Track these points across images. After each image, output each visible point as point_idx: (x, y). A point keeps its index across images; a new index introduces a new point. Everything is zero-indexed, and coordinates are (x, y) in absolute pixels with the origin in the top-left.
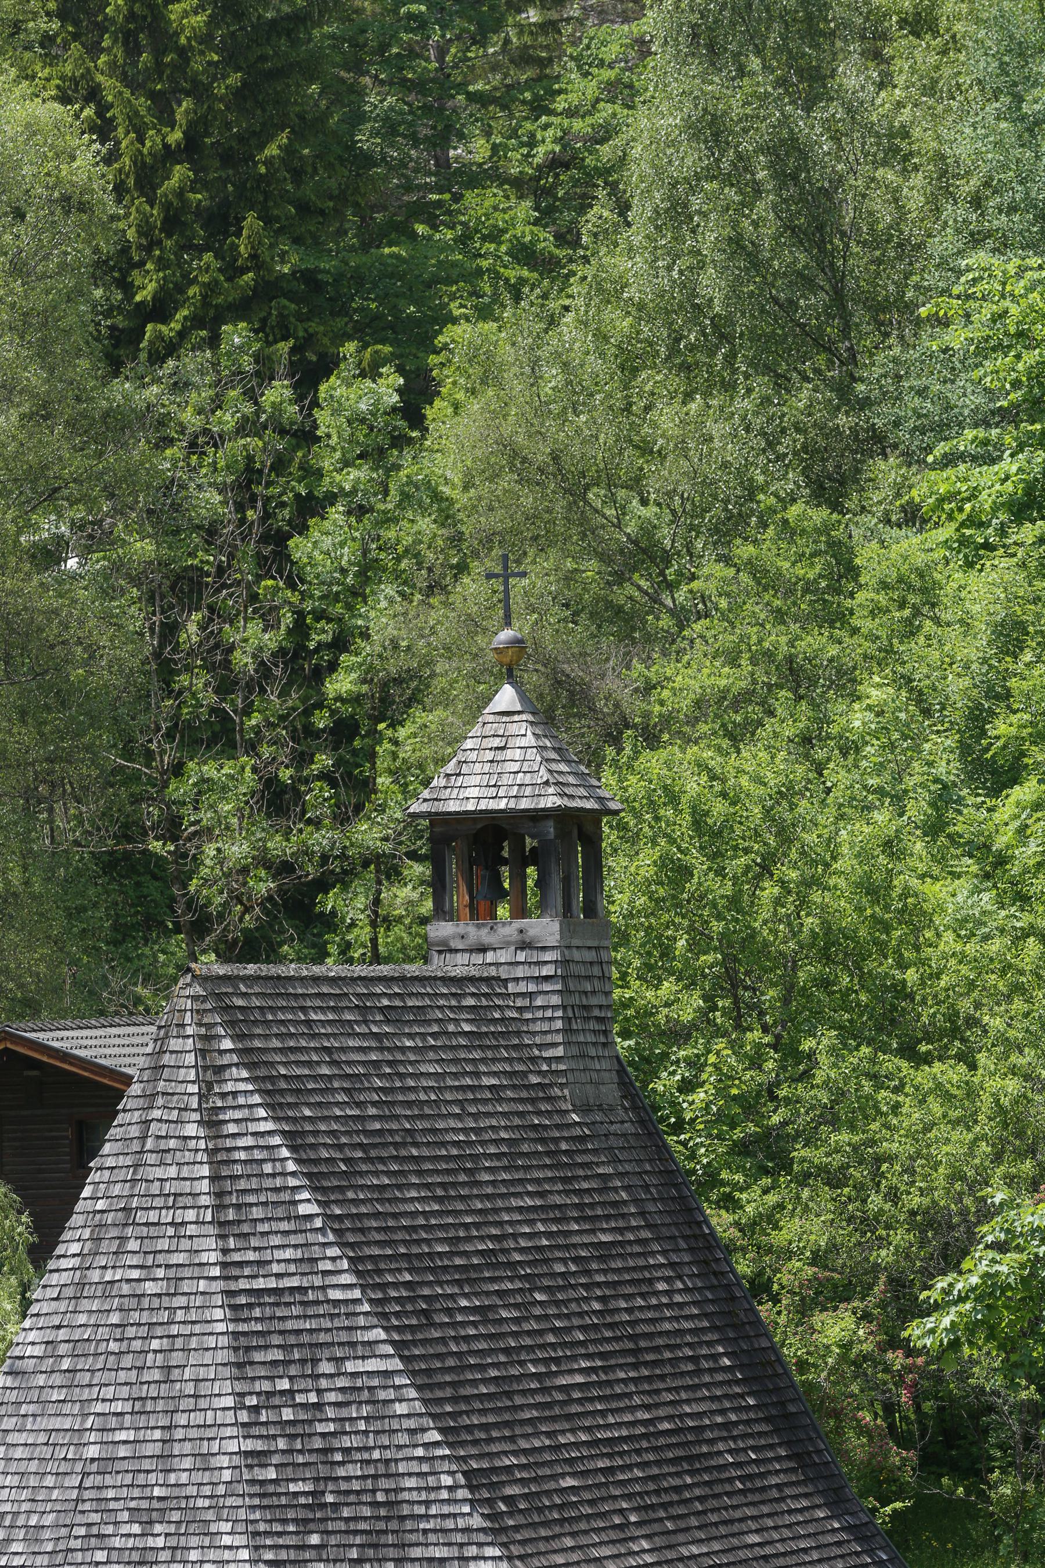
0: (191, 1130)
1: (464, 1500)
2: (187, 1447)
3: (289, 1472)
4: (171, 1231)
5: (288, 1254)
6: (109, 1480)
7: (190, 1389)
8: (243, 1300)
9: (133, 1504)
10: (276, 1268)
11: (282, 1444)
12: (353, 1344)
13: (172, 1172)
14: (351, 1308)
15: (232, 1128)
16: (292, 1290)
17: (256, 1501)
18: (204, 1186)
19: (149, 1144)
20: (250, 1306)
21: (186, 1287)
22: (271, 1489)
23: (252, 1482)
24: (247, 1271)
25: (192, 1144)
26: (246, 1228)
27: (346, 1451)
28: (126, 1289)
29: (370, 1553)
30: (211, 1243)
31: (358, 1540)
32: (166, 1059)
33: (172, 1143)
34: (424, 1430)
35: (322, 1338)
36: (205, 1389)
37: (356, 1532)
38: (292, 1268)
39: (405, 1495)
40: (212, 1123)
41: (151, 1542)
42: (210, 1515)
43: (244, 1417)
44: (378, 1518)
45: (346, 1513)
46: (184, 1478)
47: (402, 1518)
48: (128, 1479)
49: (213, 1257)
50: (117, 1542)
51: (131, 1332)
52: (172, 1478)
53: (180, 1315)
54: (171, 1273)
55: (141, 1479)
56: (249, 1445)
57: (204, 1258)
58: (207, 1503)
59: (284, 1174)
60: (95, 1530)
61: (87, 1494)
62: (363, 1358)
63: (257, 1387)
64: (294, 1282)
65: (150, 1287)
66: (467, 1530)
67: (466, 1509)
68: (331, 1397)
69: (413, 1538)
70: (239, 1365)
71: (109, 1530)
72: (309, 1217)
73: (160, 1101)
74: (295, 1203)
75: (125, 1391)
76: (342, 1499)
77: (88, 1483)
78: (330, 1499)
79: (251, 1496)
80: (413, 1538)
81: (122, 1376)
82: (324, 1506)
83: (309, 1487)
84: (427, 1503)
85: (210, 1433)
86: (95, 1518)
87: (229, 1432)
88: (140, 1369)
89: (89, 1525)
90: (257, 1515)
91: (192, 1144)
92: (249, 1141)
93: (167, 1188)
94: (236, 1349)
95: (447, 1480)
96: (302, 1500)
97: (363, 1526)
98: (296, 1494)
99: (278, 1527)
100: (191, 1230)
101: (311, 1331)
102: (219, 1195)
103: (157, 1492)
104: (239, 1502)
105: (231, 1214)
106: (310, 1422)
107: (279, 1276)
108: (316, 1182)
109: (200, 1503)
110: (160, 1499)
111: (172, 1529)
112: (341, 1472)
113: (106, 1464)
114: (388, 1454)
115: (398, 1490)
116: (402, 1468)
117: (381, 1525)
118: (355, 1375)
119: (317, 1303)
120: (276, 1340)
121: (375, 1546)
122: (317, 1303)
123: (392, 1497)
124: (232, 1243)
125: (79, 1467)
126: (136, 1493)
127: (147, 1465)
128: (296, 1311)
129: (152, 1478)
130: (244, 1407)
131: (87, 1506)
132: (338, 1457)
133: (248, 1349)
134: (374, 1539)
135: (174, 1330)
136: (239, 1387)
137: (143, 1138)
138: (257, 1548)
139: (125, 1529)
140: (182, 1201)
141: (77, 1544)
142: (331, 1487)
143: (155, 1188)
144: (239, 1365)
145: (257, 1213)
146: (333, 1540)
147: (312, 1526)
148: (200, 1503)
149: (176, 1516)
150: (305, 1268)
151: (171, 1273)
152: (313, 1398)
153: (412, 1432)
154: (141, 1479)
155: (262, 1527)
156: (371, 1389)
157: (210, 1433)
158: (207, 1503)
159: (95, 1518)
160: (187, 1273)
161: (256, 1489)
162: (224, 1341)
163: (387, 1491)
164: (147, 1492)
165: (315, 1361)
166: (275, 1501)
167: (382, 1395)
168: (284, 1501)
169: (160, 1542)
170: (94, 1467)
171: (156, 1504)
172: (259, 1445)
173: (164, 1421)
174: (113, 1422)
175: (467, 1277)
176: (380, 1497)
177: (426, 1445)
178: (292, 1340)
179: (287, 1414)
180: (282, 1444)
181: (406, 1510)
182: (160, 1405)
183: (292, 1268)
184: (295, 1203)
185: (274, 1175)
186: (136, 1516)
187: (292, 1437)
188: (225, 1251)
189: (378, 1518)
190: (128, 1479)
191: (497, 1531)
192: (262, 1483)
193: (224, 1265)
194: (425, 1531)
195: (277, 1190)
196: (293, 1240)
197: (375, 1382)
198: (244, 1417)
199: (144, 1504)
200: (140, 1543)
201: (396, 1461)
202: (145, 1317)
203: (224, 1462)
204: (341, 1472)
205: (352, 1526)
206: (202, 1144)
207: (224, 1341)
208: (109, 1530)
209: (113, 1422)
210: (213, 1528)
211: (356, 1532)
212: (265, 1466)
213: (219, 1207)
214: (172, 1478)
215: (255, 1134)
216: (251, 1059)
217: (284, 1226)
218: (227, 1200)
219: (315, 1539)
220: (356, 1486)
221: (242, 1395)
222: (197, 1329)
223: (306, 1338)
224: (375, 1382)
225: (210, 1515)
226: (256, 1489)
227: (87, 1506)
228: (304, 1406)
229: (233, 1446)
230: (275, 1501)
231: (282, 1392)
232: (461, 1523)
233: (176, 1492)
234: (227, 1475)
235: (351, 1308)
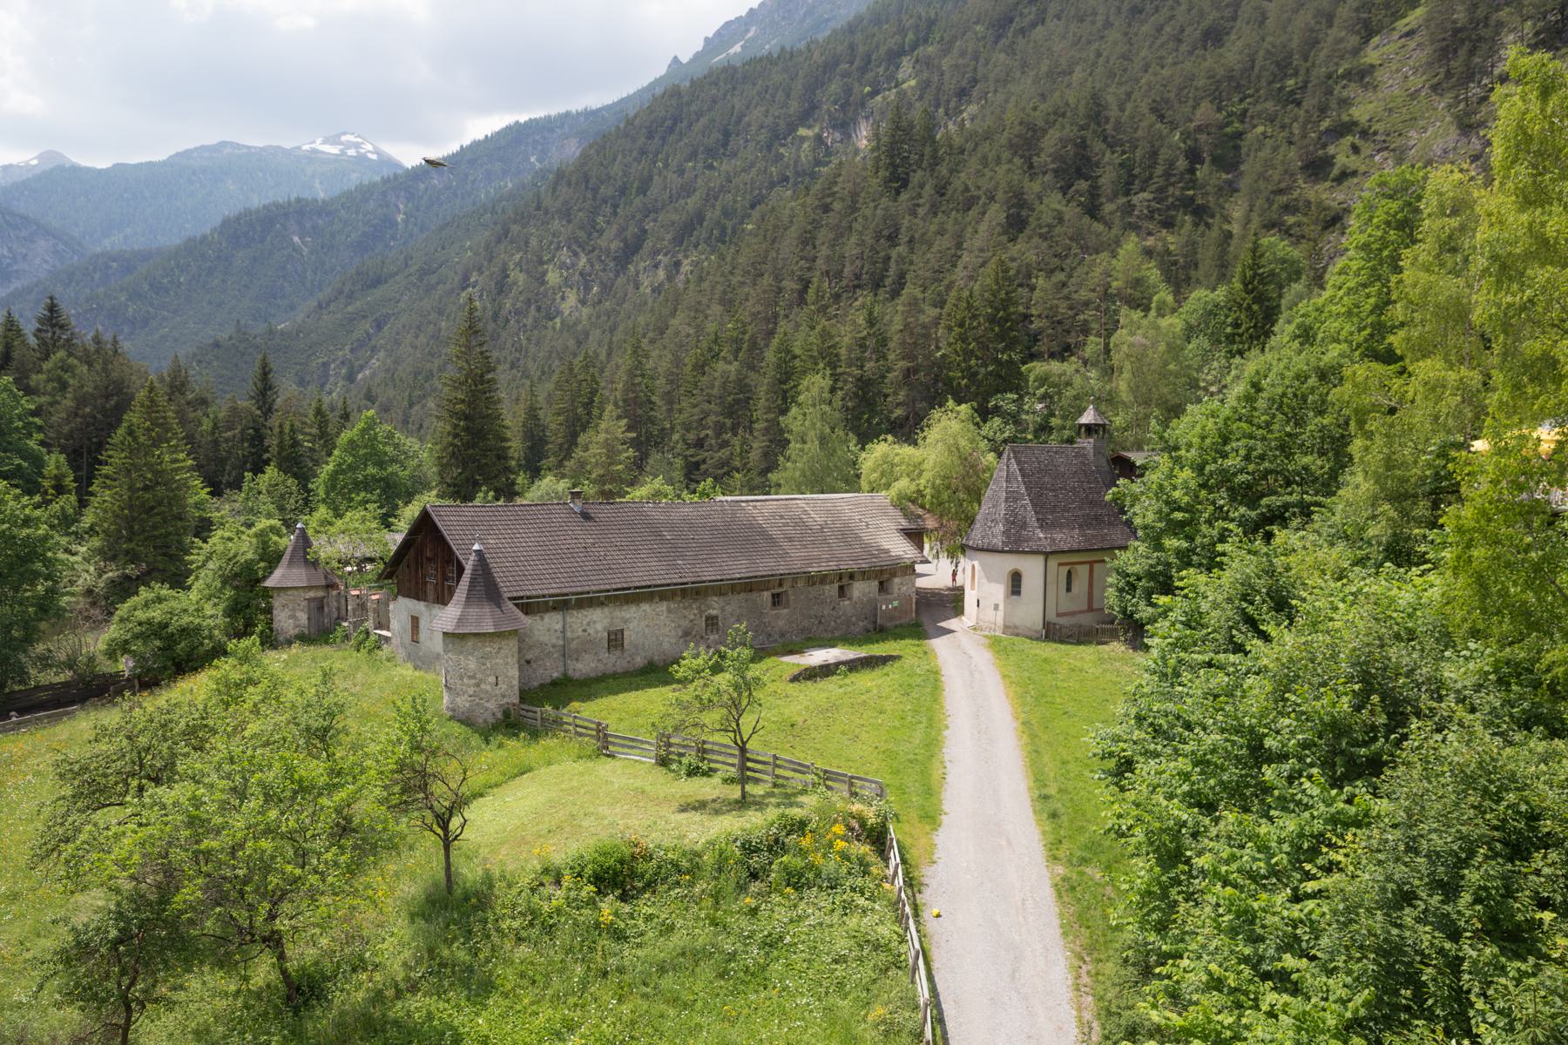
108: (1023, 476)
175: (1052, 491)
191: (1041, 527)
216: (1015, 458)
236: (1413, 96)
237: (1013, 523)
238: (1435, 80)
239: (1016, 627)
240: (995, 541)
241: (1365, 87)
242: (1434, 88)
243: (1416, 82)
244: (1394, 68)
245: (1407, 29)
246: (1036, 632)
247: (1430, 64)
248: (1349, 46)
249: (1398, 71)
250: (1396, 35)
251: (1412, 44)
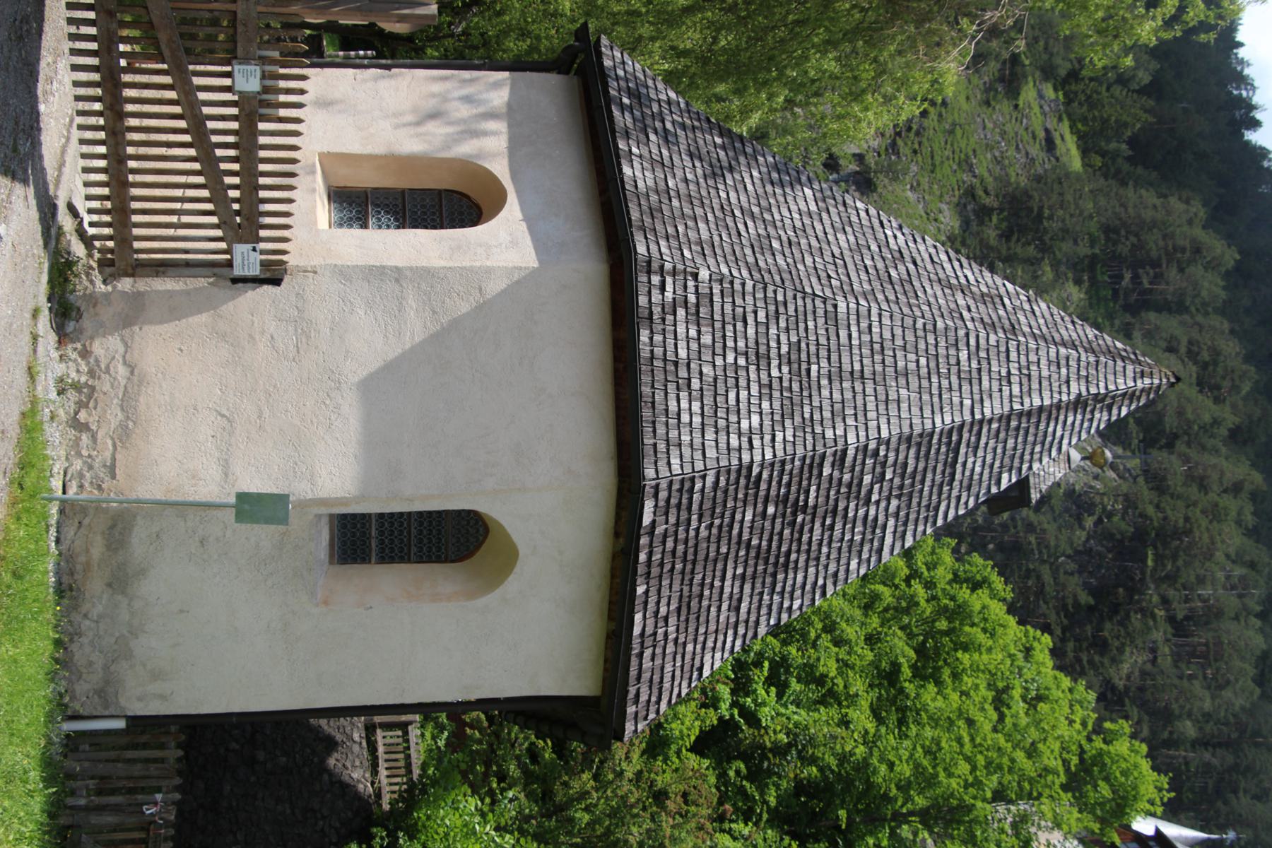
0: (1074, 388)
1: (779, 619)
2: (848, 395)
3: (824, 485)
4: (1004, 372)
5: (978, 469)
6: (821, 321)
7: (893, 396)
8: (954, 438)
9: (803, 345)
10: (971, 460)
11: (847, 477)
12: (906, 524)
13: (1045, 373)
14: (931, 520)
15: (1070, 420)
16: (953, 475)
17: (808, 461)
18: (1037, 402)
19: (1063, 351)
20: (949, 443)
21: (966, 387)
22: (815, 472)
23: (823, 456)
24: (973, 439)
25: (1064, 389)
26: (1002, 435)
27: (832, 527)
28: (961, 333)
29: (753, 554)
30: (997, 411)
31: (764, 543)
32: (1119, 363)
33: (1064, 371)
34: (835, 584)
35: (915, 501)
36: (893, 408)
37: (770, 541)
38: (967, 473)
39: (791, 575)
40: (1079, 404)
41: (775, 363)
42: (798, 419)
43: (872, 445)
44: (778, 557)
45: (787, 532)
46: (825, 393)
47: (774, 575)
48: (823, 341)
49: (987, 412)
50: (773, 331)
51: (931, 339)
52: (824, 382)
53: (945, 383)
54: (975, 374)
55: (823, 353)
56: (851, 452)
57: (987, 404)
58: (807, 416)
59: (1031, 461)
60: (782, 310)
61: (808, 301)
62: (895, 532)
63: (892, 455)
64: (958, 476)
65: (963, 355)
66: (757, 623)
67: (772, 622)
68: (872, 512)
69: (758, 585)
70: (909, 439)
71: (783, 324)
72: (999, 483)
73: (1092, 359)
74: (1010, 471)
75: (887, 335)
76: (797, 527)
77: (818, 302)
78: (799, 519)
79: (813, 457)
80: (758, 585)
81: (898, 331)
82: (794, 514)
83: (811, 501)
84: (782, 593)
85: (861, 418)
86: (791, 311)
87: (862, 434)
88: (904, 348)
89: (785, 304)
90: (797, 463)
91: (1064, 389)
92: (1059, 433)
93: (1034, 368)
94: (921, 435)
95: (796, 604)
96: (802, 497)
97: (774, 544)
98: (807, 492)
99: (786, 478)
100: (1006, 389)
101: (922, 491)
102: (1029, 414)
103: (814, 368)
104: (809, 447)
105: (1014, 423)
106: (858, 498)
107: (964, 464)
109: (807, 409)
110: (809, 371)
111: (786, 384)
112: (817, 525)
113: (832, 317)
114: (823, 559)
115: (796, 569)
116: (812, 570)
117: (772, 560)
118: (884, 527)
119: (940, 494)
120: (921, 466)
121: (757, 557)
122: (940, 494)
123: (792, 565)
124: (995, 426)
125: (828, 293)
126: (813, 349)
127: (834, 357)
128: (938, 478)
129: (824, 363)
130: (879, 444)
131: (800, 302)
132: (828, 522)
133: (919, 445)
134: (763, 555)
135: (934, 379)
136: (894, 440)
137: (1064, 345)
138: (772, 465)
139: (783, 338)
140: (1025, 380)
141: (770, 294)
142: (808, 518)
143: (1033, 358)
144: (909, 439)
145: (1011, 443)
146: (767, 524)
147: (781, 507)
148: (807, 409)
149: (796, 386)
150: (965, 483)
151: (975, 374)
152: (875, 497)
153: (836, 575)
154: (823, 353)
155: (788, 467)
156: (872, 541)
157: (861, 418)
158: (807, 416)
159: (791, 311)
160: (976, 389)
161: (817, 460)
162: (928, 426)
163: (797, 562)
164: (813, 359)
165: (899, 497)
166: (806, 475)
167: (866, 548)
168: (805, 483)
169: (775, 373)
170: (830, 308)
171: (804, 366)
172: (849, 459)
173: (867, 373)
174: (864, 324)
176: (793, 556)
177: (824, 586)
178: (918, 478)
179: (867, 479)
180: (847, 477)
181: (780, 577)
182: (879, 368)
183: (967, 473)
184: (1010, 471)
185: (1032, 453)
186: (794, 348)
187: (850, 485)
188: (990, 421)
189: (778, 557)
190: (823, 341)
192: (821, 465)
193: (981, 422)
194: (761, 594)
195: (1022, 457)
196: (986, 472)
197: (876, 544)
198: (872, 445)
199: (804, 356)
200: (773, 353)
201: (817, 566)
202: (942, 351)
203: (840, 432)
204: (817, 525)
205: (776, 538)
206: (1065, 398)
207: (928, 426)
208: (783, 324)
209: (864, 324)
210: (788, 423)
211: (770, 541)
212: (833, 465)
213: (1020, 414)
214: (824, 382)
215: (1062, 437)
217: (997, 464)
218: (1024, 420)
219: (771, 510)
220: (805, 537)
221: (888, 442)
222: (936, 399)
223: (918, 487)
224: (876, 544)
225: (798, 419)
226: (817, 460)
227: (800, 302)
228: (870, 492)
229: (851, 439)
230: (806, 475)
231: (883, 474)
232: (763, 619)
233: (814, 387)
234: (829, 434)
235: (931, 520)
236: (966, 165)
237: (792, 506)
238: (980, 193)
239: (120, 582)
240: (689, 408)
241: (989, 89)
242: (970, 193)
243: (983, 165)
244: (1008, 128)
245: (1056, 136)
246: (103, 693)
247: (1003, 180)
248: (1058, 61)
249: (1003, 133)
250: (1052, 123)
251: (1035, 151)
